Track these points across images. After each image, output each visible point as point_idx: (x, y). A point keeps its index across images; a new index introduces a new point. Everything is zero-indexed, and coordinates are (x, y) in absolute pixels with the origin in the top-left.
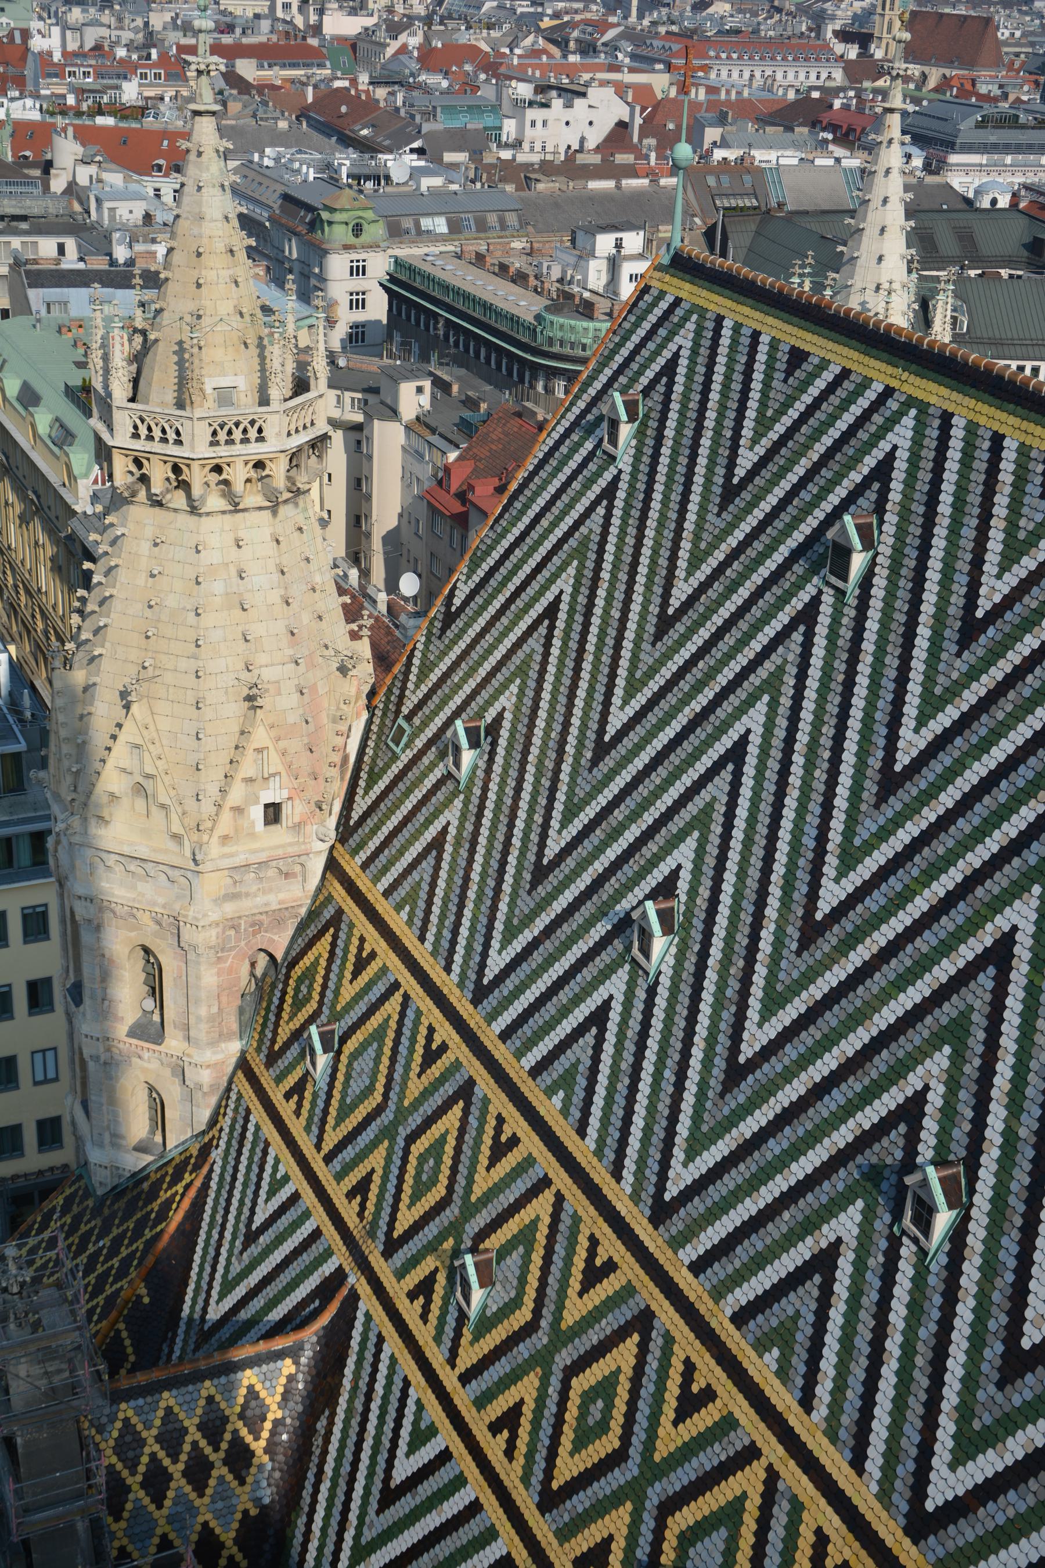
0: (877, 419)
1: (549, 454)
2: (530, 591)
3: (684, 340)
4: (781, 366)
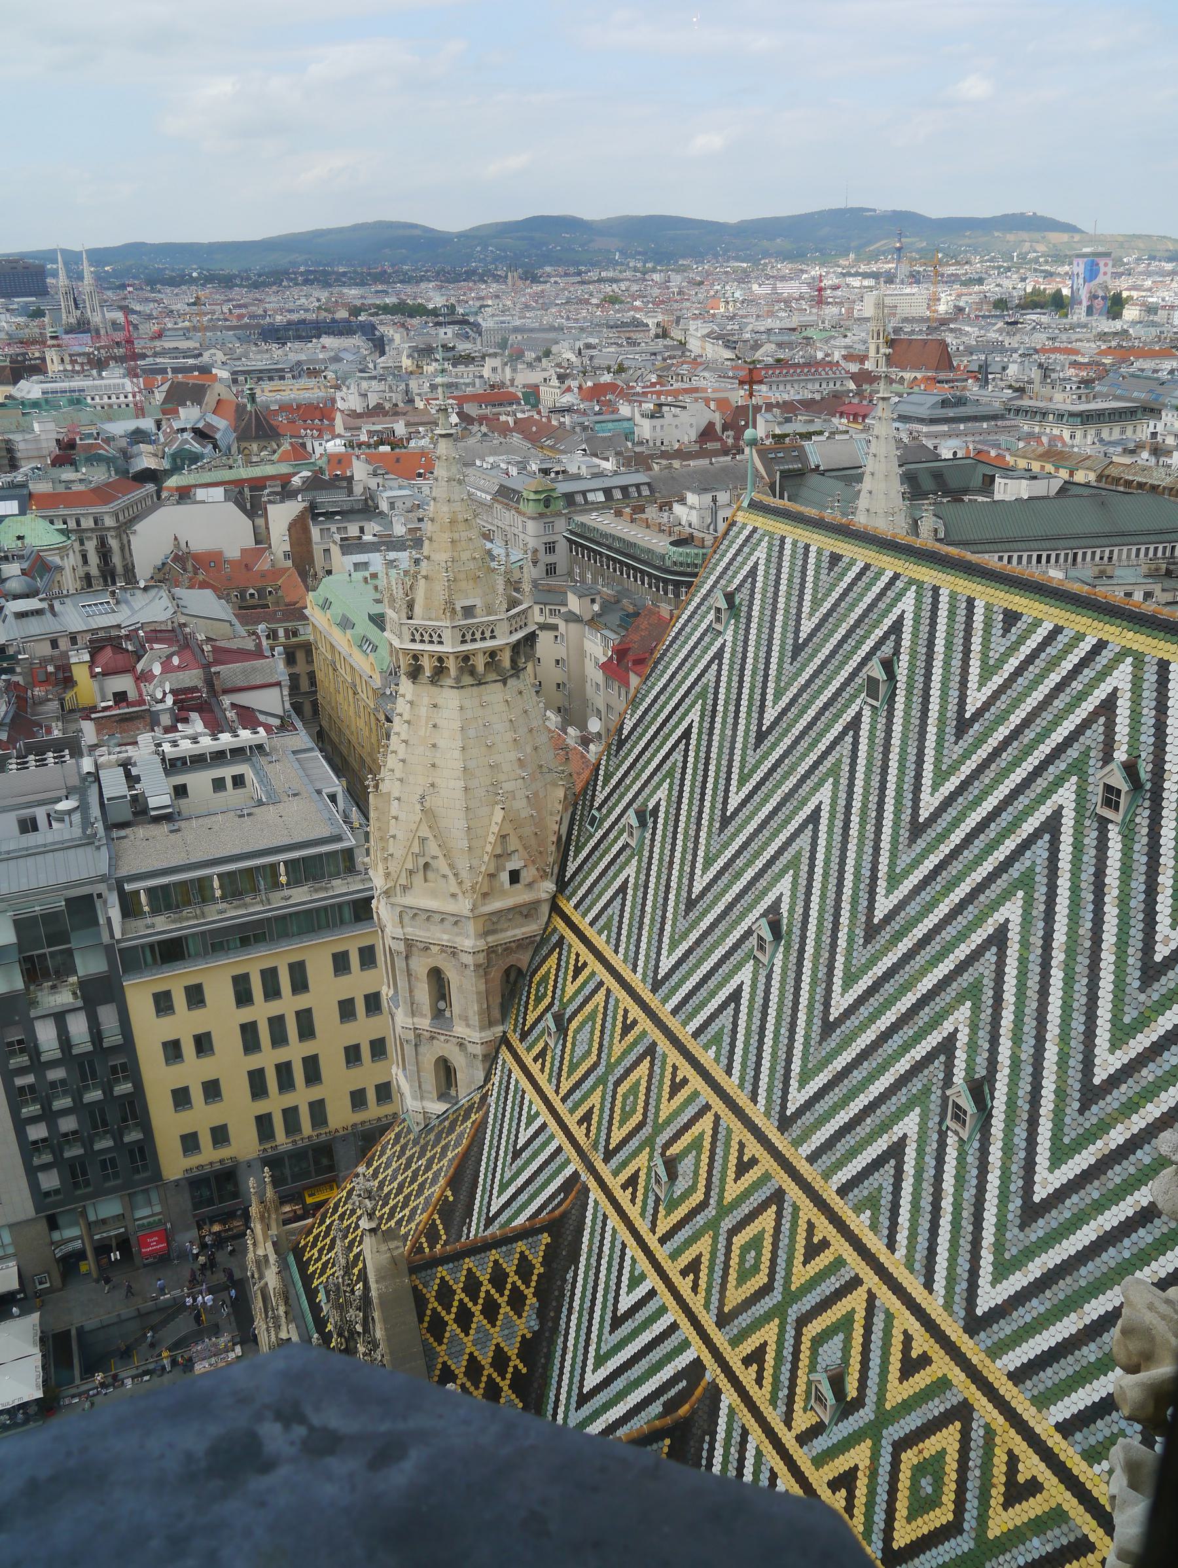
0: (891, 594)
1: (679, 633)
2: (672, 722)
3: (761, 554)
4: (825, 565)
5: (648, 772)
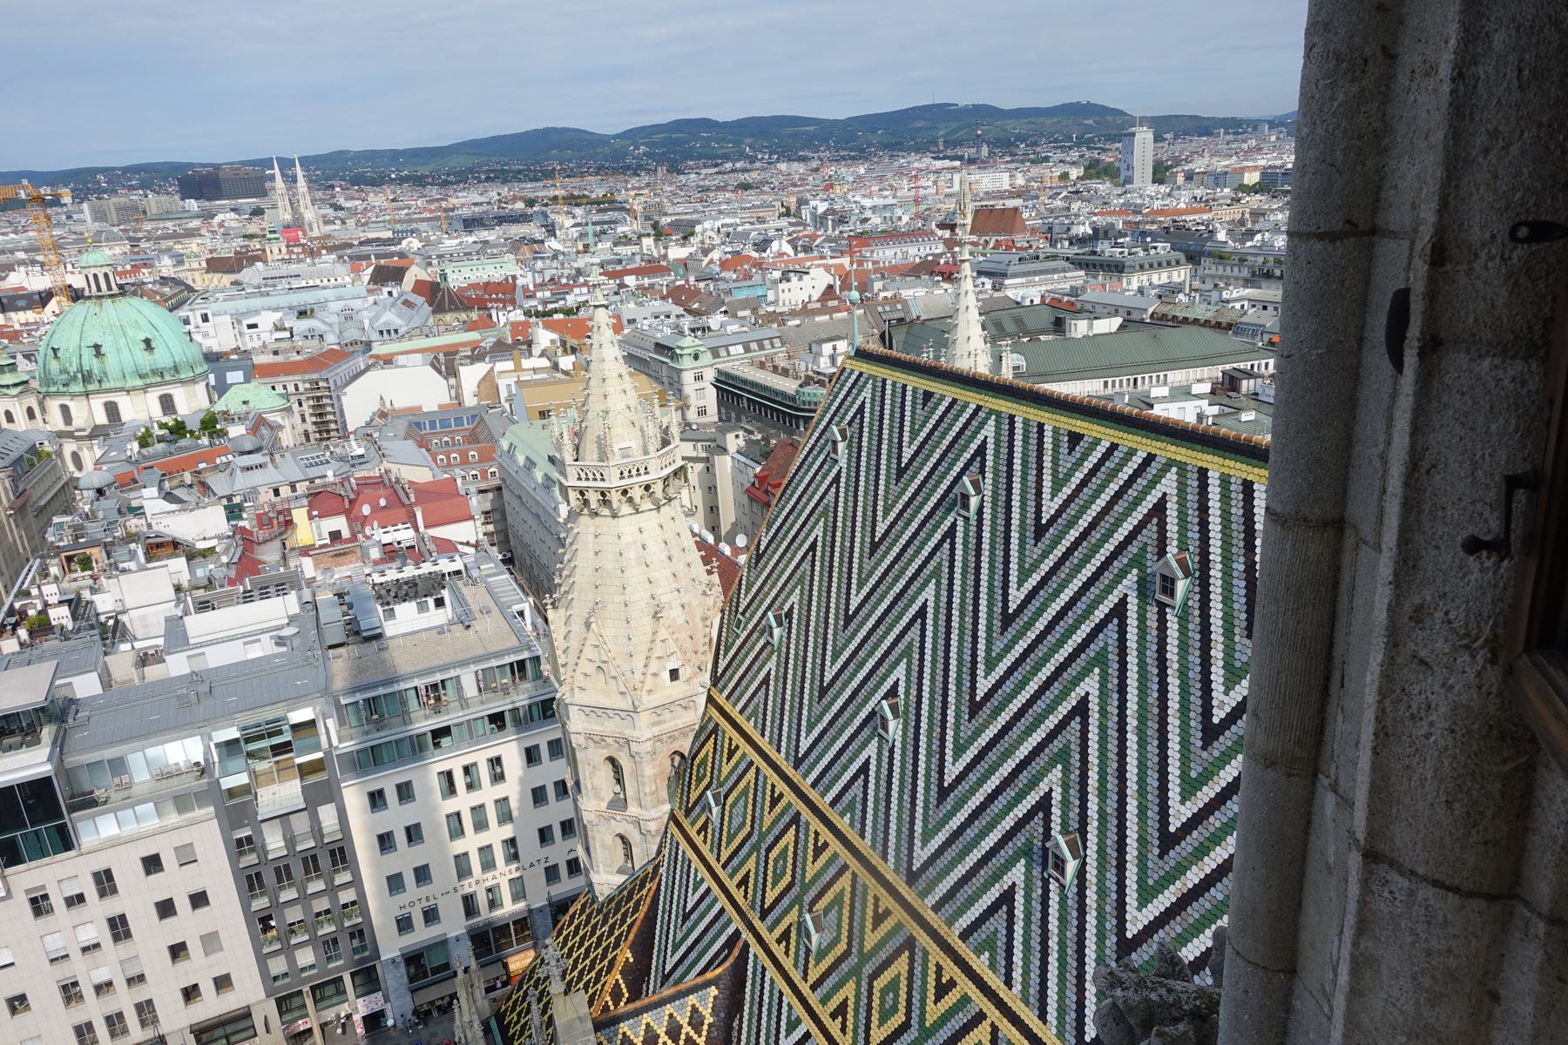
0: (975, 423)
3: (867, 394)
4: (920, 401)
5: (782, 581)
